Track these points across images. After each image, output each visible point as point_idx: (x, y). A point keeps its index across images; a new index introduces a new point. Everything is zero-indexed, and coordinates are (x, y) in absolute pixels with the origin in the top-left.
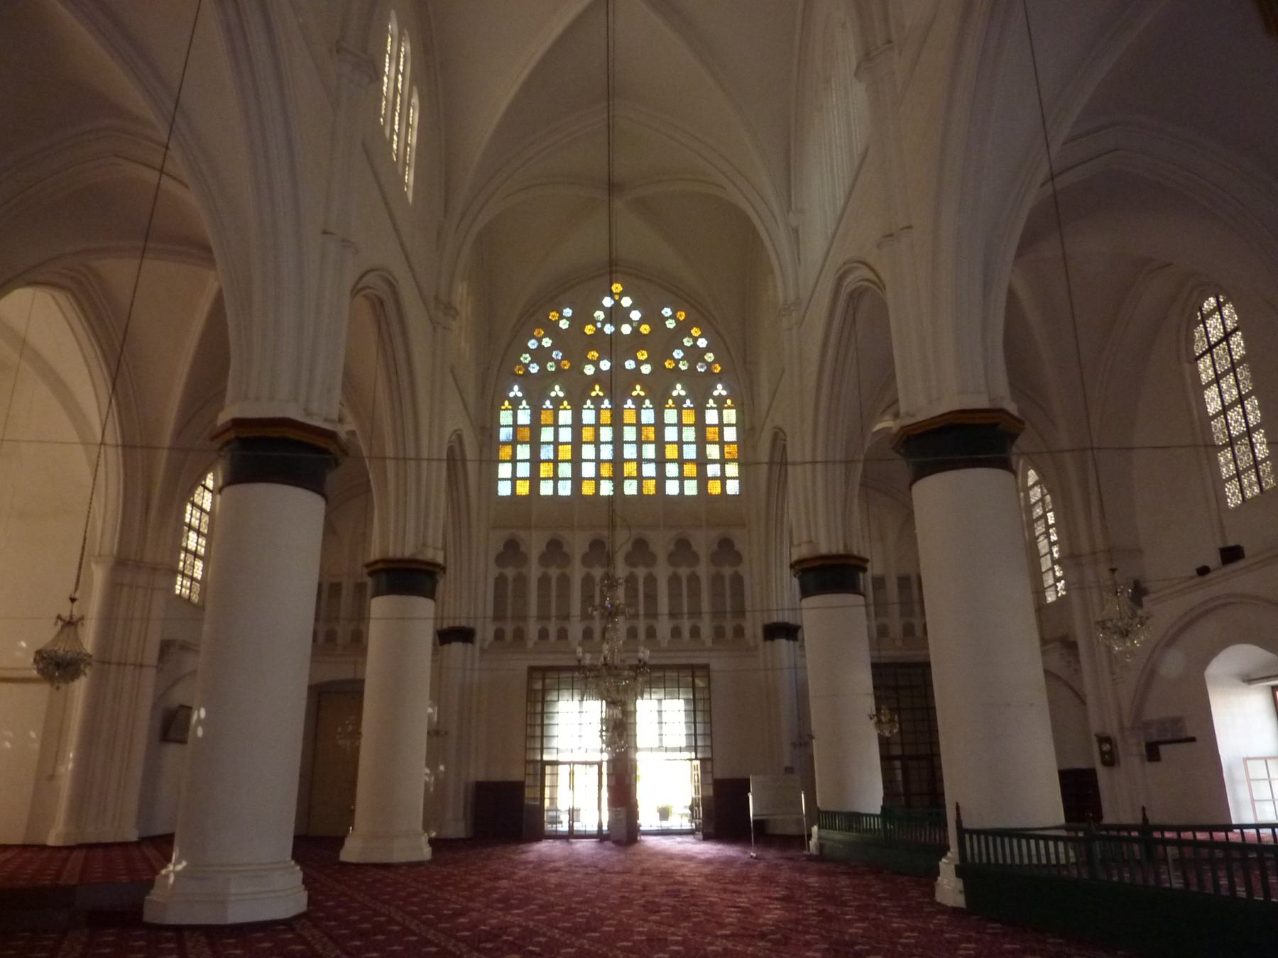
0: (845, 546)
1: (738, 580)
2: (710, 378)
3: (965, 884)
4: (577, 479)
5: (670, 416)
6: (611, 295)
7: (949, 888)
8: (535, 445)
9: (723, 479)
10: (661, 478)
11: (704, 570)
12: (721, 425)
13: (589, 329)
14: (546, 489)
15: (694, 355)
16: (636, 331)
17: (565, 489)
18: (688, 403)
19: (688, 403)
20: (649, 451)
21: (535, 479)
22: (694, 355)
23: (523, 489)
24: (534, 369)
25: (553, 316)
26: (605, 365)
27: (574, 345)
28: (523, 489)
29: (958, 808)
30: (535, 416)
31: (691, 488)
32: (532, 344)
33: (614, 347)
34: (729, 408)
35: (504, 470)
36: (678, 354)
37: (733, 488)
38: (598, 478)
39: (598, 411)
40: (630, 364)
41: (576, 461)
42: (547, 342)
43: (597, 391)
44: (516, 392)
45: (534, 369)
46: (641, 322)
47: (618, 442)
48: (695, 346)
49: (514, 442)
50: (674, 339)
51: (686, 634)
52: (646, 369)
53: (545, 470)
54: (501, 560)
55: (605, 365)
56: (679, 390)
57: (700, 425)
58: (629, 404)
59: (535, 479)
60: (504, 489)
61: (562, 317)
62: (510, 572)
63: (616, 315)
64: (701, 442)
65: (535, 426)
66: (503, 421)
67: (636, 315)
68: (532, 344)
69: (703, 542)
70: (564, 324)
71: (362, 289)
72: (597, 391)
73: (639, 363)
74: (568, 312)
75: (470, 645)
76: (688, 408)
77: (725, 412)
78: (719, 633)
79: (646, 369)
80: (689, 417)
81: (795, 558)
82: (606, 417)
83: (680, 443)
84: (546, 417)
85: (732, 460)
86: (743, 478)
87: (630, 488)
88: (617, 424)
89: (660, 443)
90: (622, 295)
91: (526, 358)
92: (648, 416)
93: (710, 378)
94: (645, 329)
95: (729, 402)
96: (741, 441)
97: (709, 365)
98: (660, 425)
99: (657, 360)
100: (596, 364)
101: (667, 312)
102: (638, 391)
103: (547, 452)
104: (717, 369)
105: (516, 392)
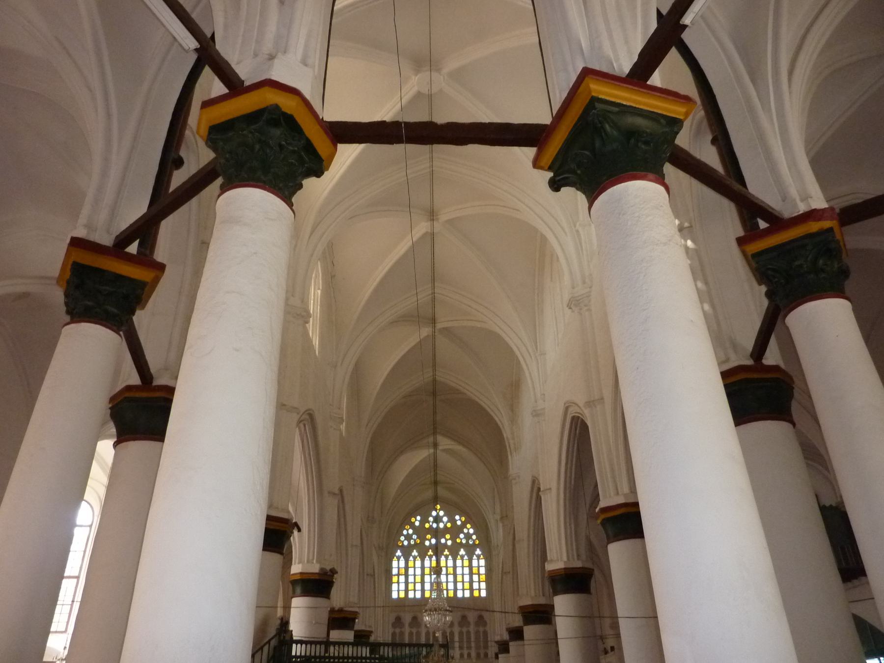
1: (485, 633)
2: (474, 546)
5: (459, 562)
6: (436, 510)
8: (407, 575)
9: (479, 590)
10: (455, 590)
11: (472, 629)
13: (427, 525)
14: (411, 595)
15: (468, 536)
16: (445, 525)
18: (466, 557)
21: (407, 591)
22: (468, 536)
23: (402, 595)
26: (433, 541)
27: (421, 532)
28: (402, 595)
33: (437, 533)
35: (395, 587)
37: (484, 594)
39: (431, 561)
42: (411, 531)
43: (430, 553)
44: (399, 553)
45: (406, 543)
49: (398, 575)
50: (460, 529)
51: (466, 656)
52: (449, 543)
54: (394, 625)
56: (462, 552)
57: (471, 567)
59: (407, 591)
62: (398, 630)
63: (437, 519)
64: (471, 574)
65: (407, 568)
67: (445, 519)
70: (417, 523)
72: (430, 553)
73: (447, 540)
74: (419, 518)
78: (478, 655)
80: (466, 563)
84: (411, 564)
89: (455, 575)
91: (402, 538)
92: (450, 563)
94: (449, 525)
96: (487, 574)
97: (474, 541)
98: (455, 567)
99: (453, 539)
100: (430, 540)
101: (457, 517)
102: (446, 552)
103: (411, 579)
104: (477, 542)
105: (399, 553)
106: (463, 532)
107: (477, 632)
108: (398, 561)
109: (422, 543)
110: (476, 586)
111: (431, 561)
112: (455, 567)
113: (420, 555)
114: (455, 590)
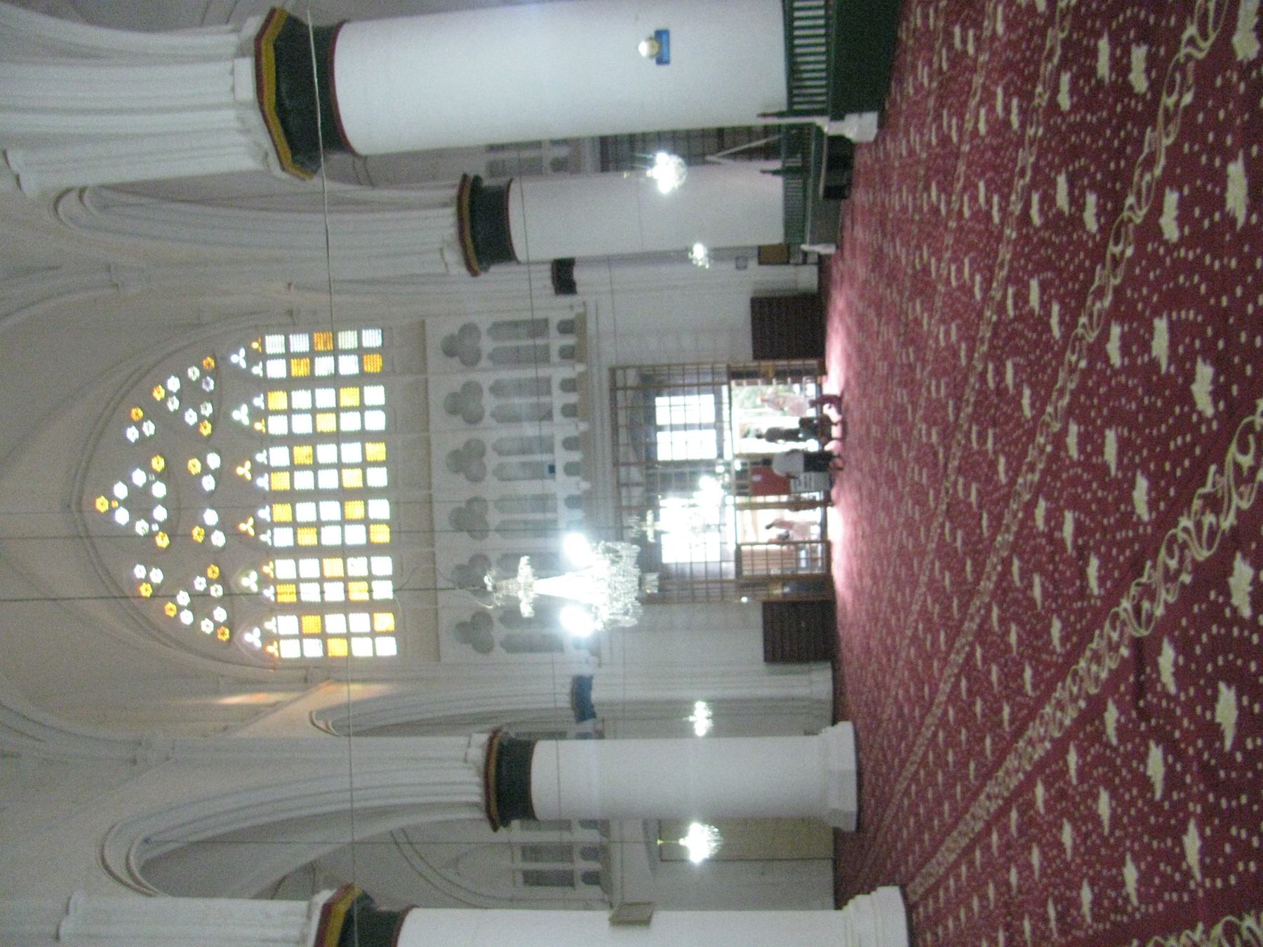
0: (445, 205)
1: (498, 329)
2: (221, 371)
3: (852, 112)
4: (370, 549)
5: (277, 426)
7: (858, 127)
9: (361, 352)
10: (363, 436)
12: (288, 356)
13: (163, 541)
14: (384, 591)
15: (191, 394)
16: (160, 476)
17: (383, 565)
18: (258, 402)
19: (258, 402)
20: (327, 453)
21: (371, 606)
22: (191, 394)
23: (386, 621)
24: (220, 614)
25: (146, 590)
28: (386, 621)
29: (764, 115)
30: (286, 609)
31: (375, 395)
32: (187, 618)
34: (263, 345)
35: (362, 649)
36: (191, 417)
37: (372, 338)
38: (367, 522)
39: (273, 525)
40: (208, 483)
41: (344, 551)
42: (183, 598)
43: (247, 527)
44: (252, 638)
46: (148, 470)
47: (316, 495)
48: (179, 395)
49: (323, 636)
50: (169, 423)
53: (359, 592)
55: (211, 517)
56: (241, 415)
57: (289, 384)
58: (262, 482)
59: (371, 606)
60: (388, 647)
61: (147, 580)
64: (311, 382)
65: (300, 608)
66: (296, 654)
68: (187, 618)
69: (446, 379)
71: (132, 875)
72: (247, 527)
73: (206, 470)
74: (140, 571)
75: (594, 681)
76: (266, 401)
77: (269, 350)
79: (214, 461)
80: (278, 400)
81: (463, 270)
82: (282, 512)
83: (314, 411)
85: (335, 340)
86: (359, 325)
87: (378, 478)
88: (292, 497)
89: (315, 438)
90: (111, 497)
92: (279, 456)
93: (221, 371)
94: (158, 464)
95: (255, 345)
96: (309, 329)
98: (291, 440)
99: (201, 446)
101: (132, 434)
102: (244, 471)
104: (209, 362)
105: (252, 638)
106: (179, 414)
107: (498, 359)
108: (278, 638)
109: (216, 556)
110: (349, 366)
111: (273, 525)
112: (291, 440)
113: (257, 566)
114: (363, 436)
